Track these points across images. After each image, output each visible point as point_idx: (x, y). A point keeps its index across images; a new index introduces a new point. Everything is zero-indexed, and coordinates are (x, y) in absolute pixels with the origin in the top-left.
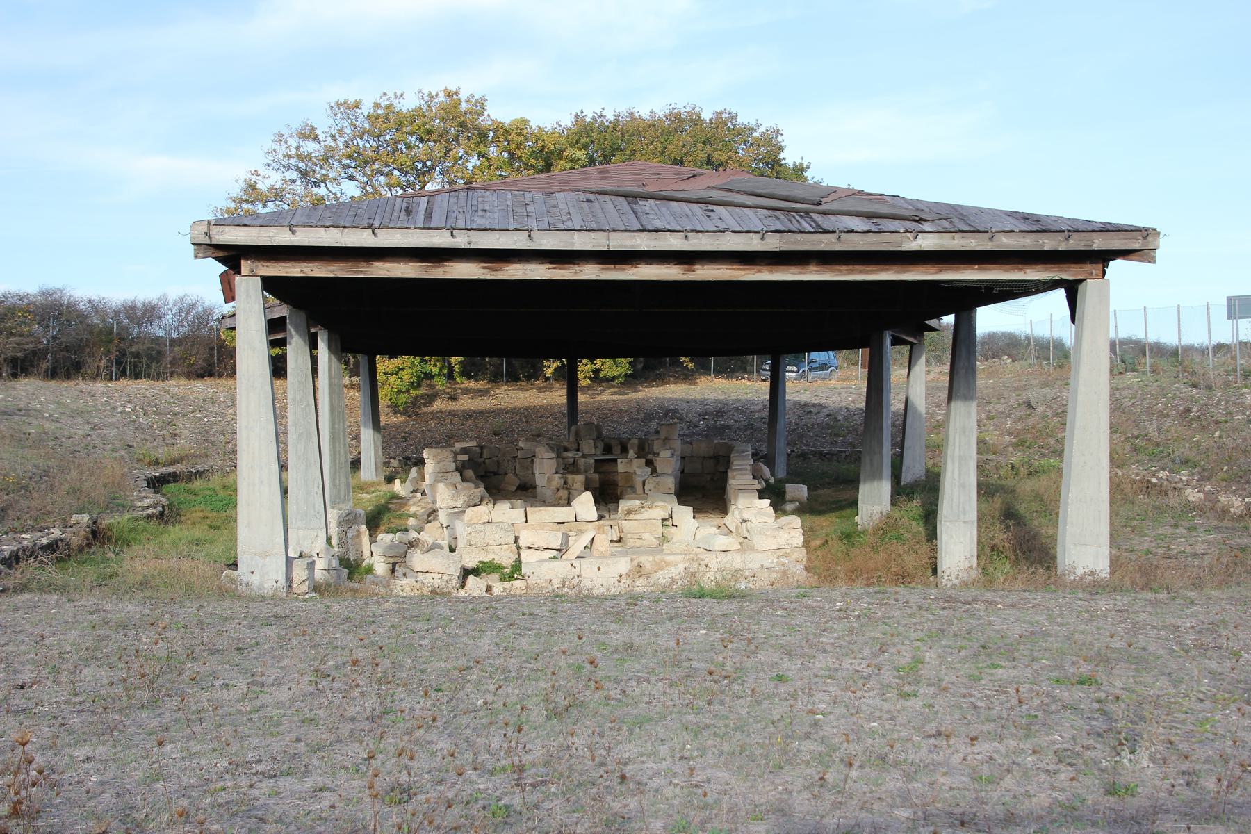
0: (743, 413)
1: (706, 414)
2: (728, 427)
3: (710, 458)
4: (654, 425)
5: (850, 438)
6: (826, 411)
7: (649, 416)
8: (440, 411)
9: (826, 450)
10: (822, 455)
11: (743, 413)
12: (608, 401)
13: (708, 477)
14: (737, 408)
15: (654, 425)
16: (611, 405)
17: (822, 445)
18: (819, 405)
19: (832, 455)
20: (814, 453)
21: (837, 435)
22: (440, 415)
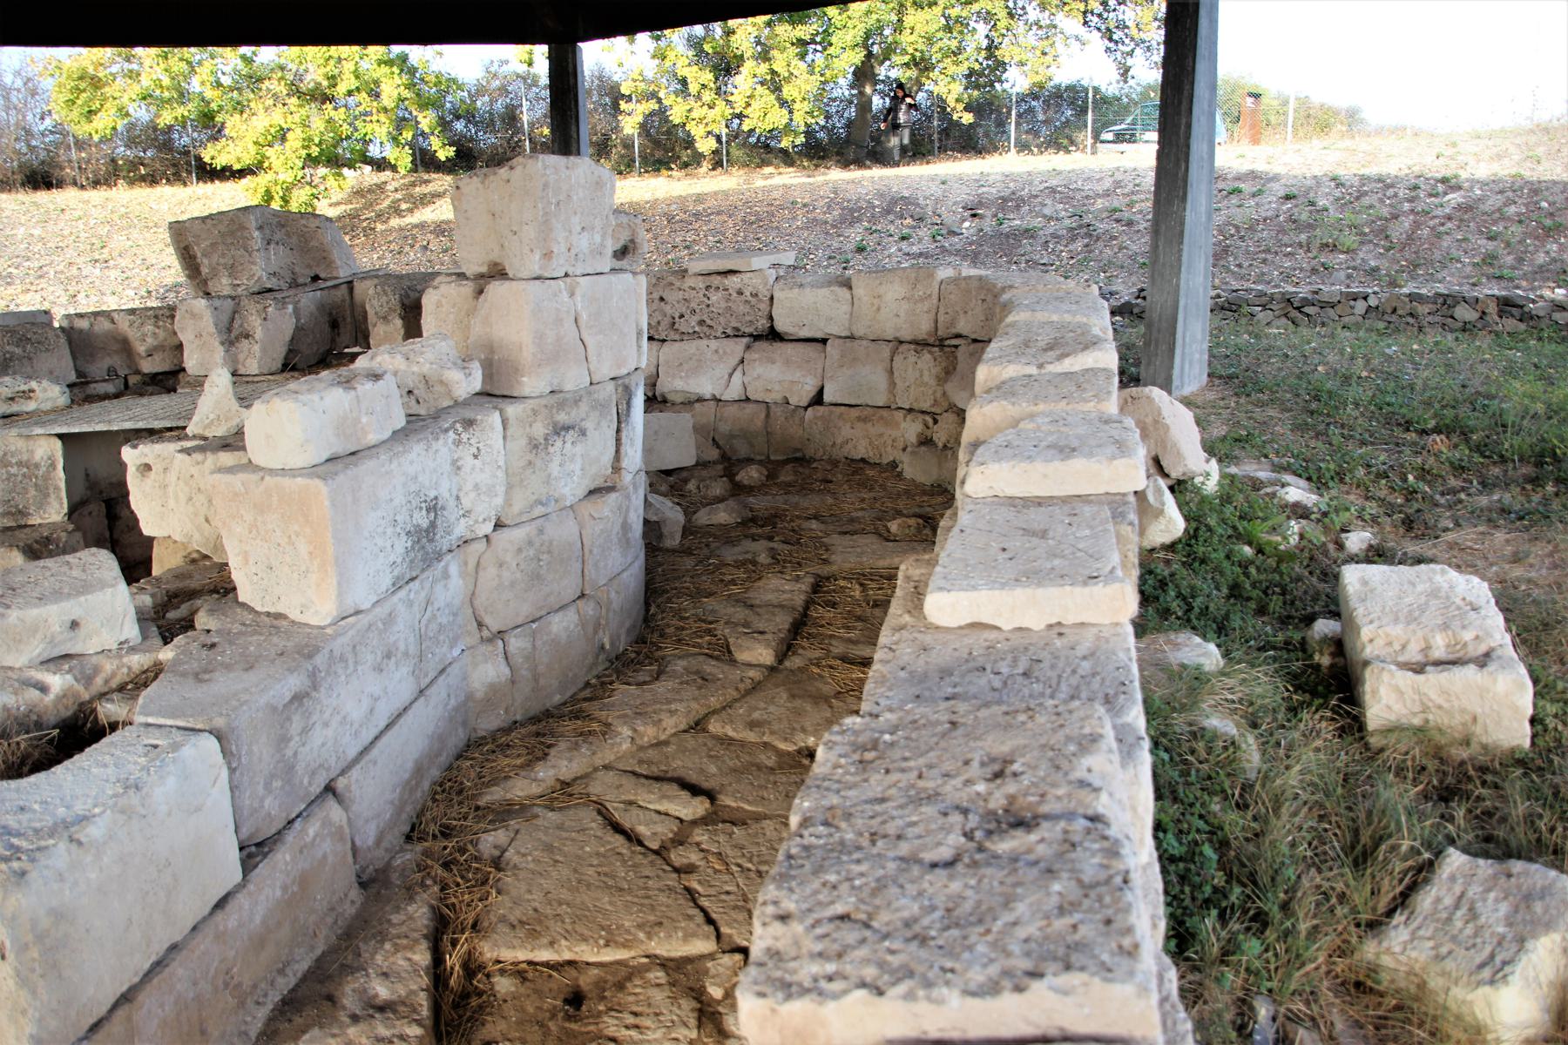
0: (1067, 199)
1: (980, 204)
2: (1029, 233)
3: (920, 344)
4: (856, 234)
5: (1370, 257)
6: (1279, 189)
7: (851, 215)
8: (422, 226)
9: (1303, 291)
10: (1294, 309)
11: (1067, 199)
12: (777, 187)
13: (911, 430)
14: (1053, 191)
15: (856, 234)
16: (775, 194)
17: (1287, 277)
18: (1253, 175)
19: (1323, 305)
20: (1266, 302)
21: (1333, 248)
22: (407, 235)
